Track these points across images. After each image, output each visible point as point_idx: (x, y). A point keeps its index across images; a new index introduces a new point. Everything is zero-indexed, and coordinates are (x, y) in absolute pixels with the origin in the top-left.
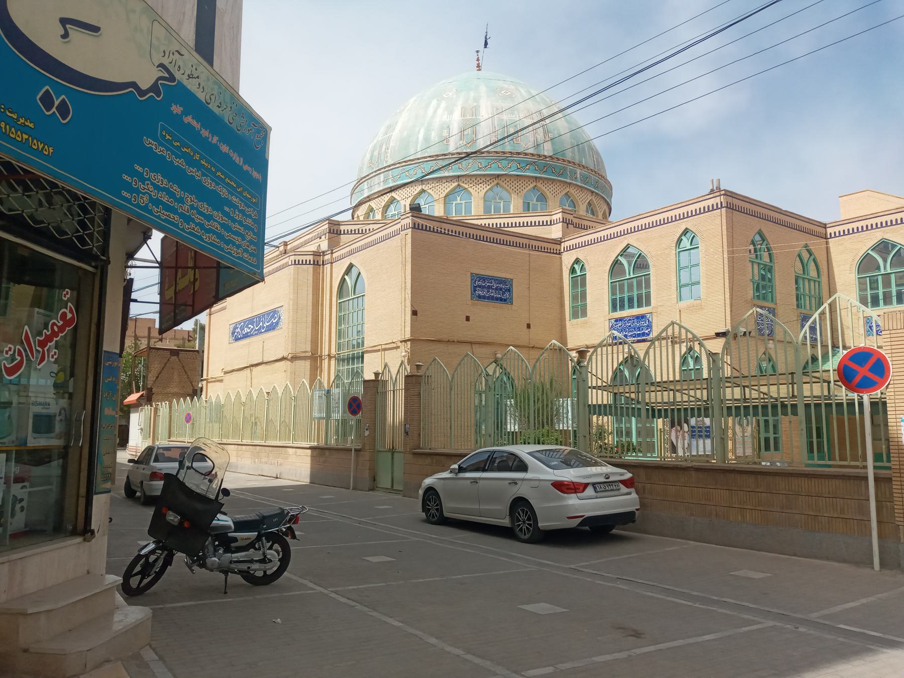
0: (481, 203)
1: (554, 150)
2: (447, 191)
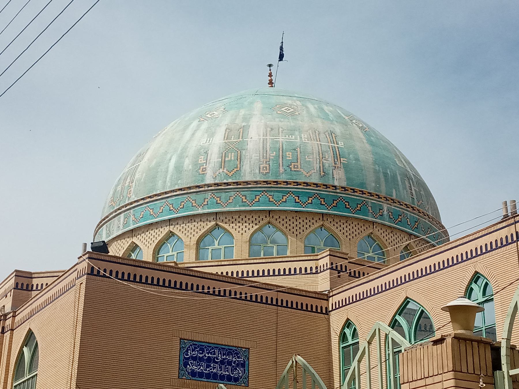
0: (246, 247)
1: (348, 179)
2: (200, 233)
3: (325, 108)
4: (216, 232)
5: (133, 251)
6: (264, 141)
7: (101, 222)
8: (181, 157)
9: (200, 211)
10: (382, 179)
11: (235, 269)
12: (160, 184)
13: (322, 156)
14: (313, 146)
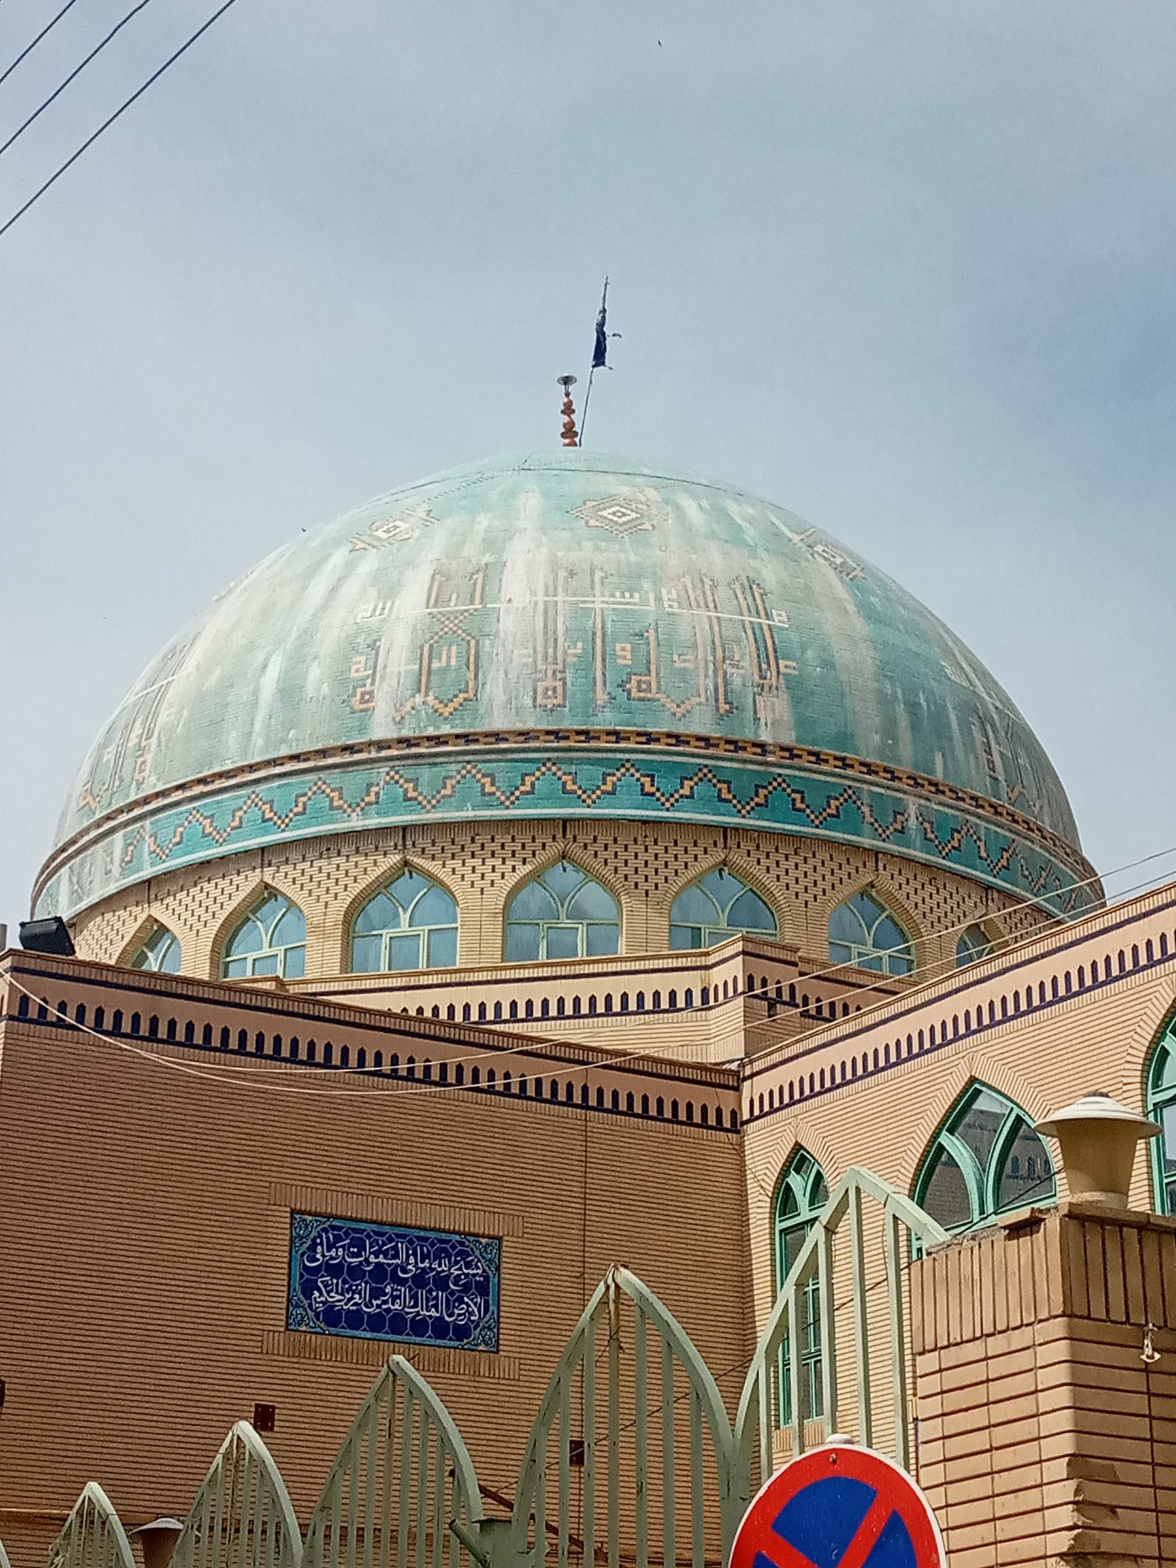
1: (801, 723)
2: (356, 889)
3: (733, 508)
4: (403, 885)
5: (152, 944)
6: (549, 611)
7: (53, 858)
8: (298, 660)
9: (356, 822)
10: (903, 721)
11: (458, 997)
12: (232, 738)
13: (722, 655)
14: (695, 623)
